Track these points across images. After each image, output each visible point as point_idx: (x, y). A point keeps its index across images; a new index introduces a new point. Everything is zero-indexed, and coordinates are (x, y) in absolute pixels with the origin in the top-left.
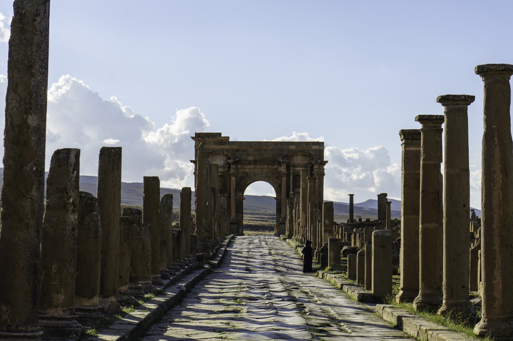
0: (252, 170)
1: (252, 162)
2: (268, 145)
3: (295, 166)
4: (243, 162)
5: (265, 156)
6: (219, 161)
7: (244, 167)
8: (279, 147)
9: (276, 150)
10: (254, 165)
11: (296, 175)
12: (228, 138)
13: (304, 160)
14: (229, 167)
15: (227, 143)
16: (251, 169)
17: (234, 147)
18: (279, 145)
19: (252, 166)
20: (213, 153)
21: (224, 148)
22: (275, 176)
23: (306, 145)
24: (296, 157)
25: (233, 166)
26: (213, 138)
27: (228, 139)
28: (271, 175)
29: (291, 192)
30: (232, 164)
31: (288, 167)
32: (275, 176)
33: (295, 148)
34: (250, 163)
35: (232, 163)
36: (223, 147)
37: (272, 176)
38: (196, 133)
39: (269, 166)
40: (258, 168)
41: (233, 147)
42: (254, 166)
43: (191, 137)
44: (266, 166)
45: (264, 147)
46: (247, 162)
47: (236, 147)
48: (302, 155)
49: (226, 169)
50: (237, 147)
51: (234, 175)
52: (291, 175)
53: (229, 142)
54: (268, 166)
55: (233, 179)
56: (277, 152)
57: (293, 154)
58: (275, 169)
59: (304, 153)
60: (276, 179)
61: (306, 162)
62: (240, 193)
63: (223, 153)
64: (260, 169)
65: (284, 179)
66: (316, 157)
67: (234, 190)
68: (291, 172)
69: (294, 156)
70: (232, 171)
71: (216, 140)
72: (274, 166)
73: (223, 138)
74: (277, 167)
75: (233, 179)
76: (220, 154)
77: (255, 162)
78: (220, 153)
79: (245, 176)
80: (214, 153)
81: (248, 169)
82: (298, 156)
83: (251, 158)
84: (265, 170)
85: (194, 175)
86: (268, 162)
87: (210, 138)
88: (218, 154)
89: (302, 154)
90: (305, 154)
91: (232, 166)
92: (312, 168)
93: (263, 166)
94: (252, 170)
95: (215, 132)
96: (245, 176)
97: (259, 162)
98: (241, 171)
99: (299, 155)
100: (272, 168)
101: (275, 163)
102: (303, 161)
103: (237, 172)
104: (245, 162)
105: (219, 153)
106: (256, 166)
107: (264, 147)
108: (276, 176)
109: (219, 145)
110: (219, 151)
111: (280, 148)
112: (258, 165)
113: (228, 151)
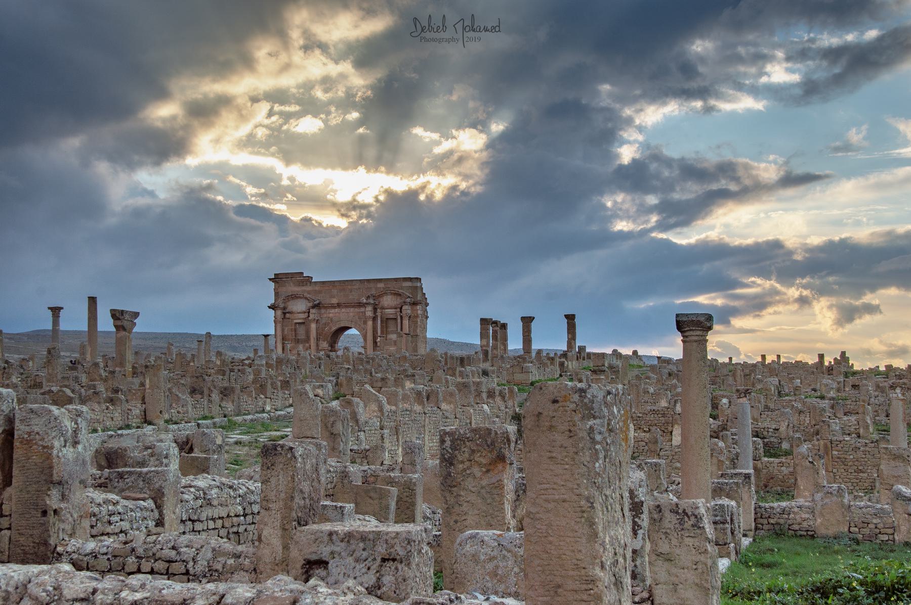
3: (383, 308)
6: (299, 306)
11: (387, 319)
19: (337, 310)
21: (305, 291)
31: (375, 310)
34: (333, 307)
36: (304, 288)
39: (356, 309)
44: (352, 309)
52: (379, 318)
55: (313, 326)
65: (370, 323)
68: (379, 314)
70: (312, 316)
75: (313, 326)
77: (339, 305)
80: (294, 297)
85: (60, 315)
91: (311, 310)
98: (325, 316)
100: (359, 311)
113: (309, 293)
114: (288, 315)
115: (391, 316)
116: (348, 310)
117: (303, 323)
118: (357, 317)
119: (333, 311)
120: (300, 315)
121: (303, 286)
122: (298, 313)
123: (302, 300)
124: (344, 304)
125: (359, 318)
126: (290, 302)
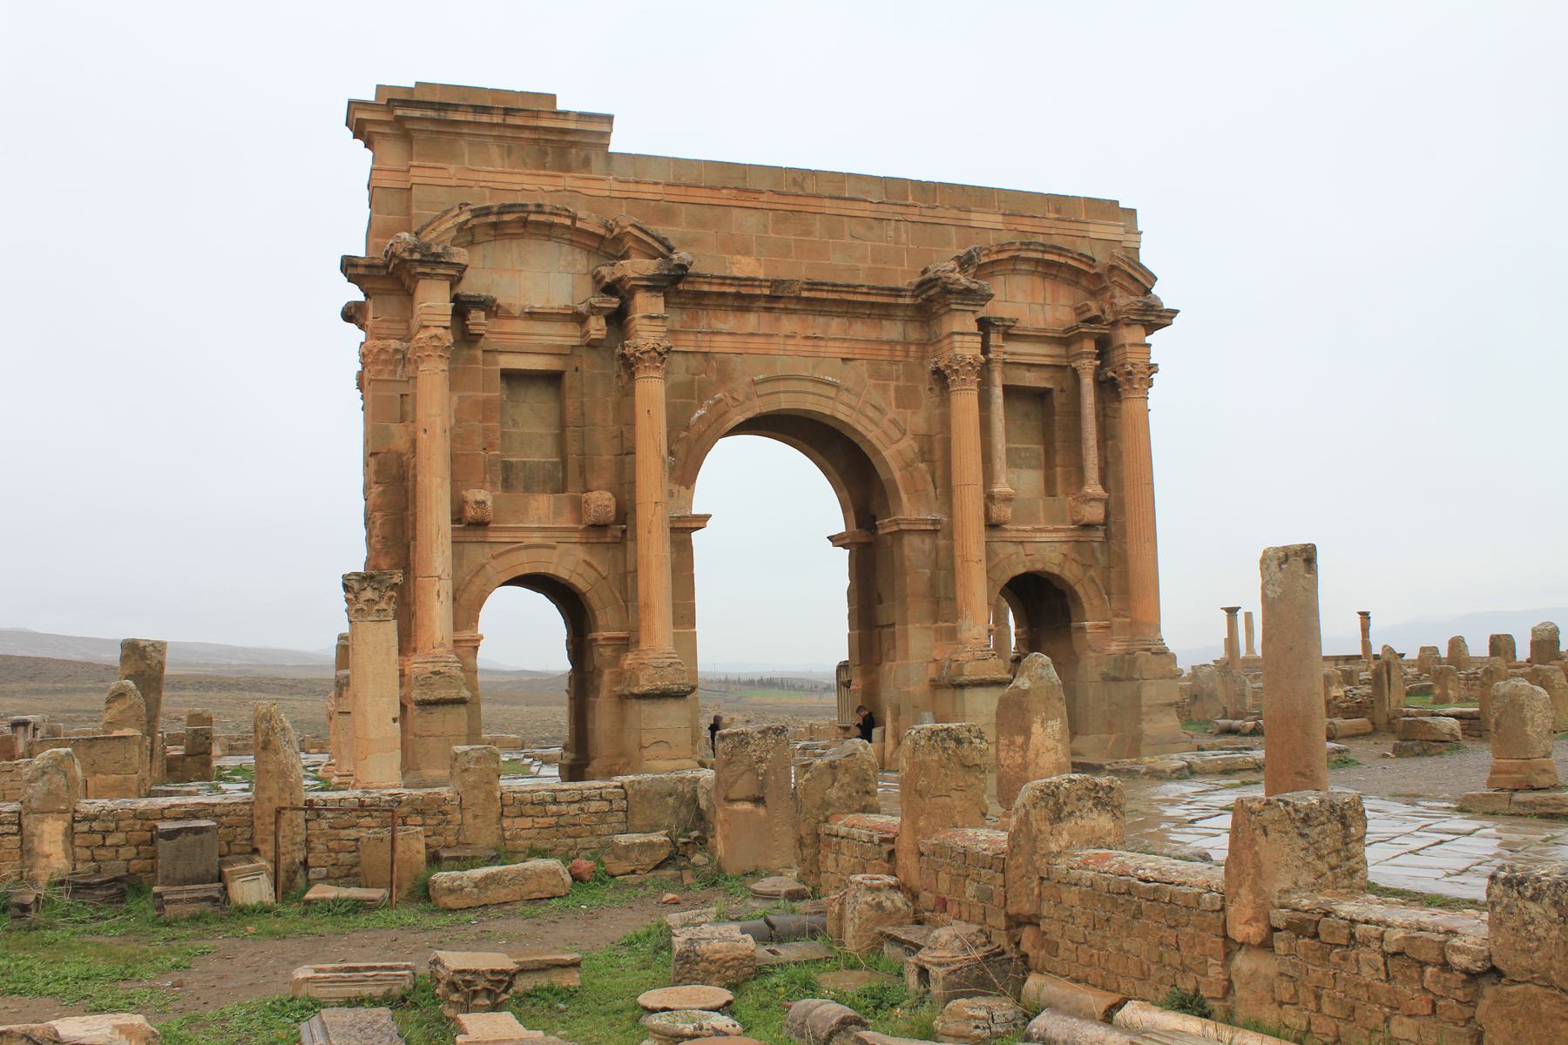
1: (758, 291)
2: (847, 195)
4: (706, 288)
5: (837, 258)
7: (703, 324)
8: (912, 210)
9: (896, 230)
12: (605, 128)
13: (1048, 301)
14: (618, 319)
15: (597, 164)
16: (752, 334)
17: (643, 188)
18: (910, 198)
19: (751, 321)
20: (507, 218)
22: (893, 384)
23: (1058, 211)
24: (1001, 278)
25: (646, 305)
26: (511, 120)
28: (872, 382)
29: (1001, 488)
30: (648, 289)
32: (893, 384)
33: (1000, 226)
34: (741, 298)
35: (648, 279)
36: (569, 181)
37: (876, 385)
38: (379, 87)
39: (860, 329)
41: (632, 187)
42: (765, 316)
44: (835, 326)
45: (827, 202)
46: (732, 290)
47: (652, 188)
48: (1032, 273)
49: (597, 327)
50: (660, 189)
53: (610, 156)
54: (850, 325)
56: (903, 238)
57: (995, 257)
58: (889, 342)
59: (1055, 258)
60: (898, 406)
61: (1058, 314)
63: (574, 218)
64: (807, 338)
65: (965, 401)
66: (1137, 276)
69: (992, 274)
71: (526, 135)
72: (885, 323)
73: (572, 126)
74: (901, 330)
75: (652, 390)
76: (547, 231)
78: (557, 220)
79: (714, 377)
81: (730, 334)
82: (1014, 271)
83: (745, 266)
84: (836, 349)
87: (485, 119)
88: (537, 223)
89: (1037, 261)
90: (1062, 260)
92: (1104, 347)
93: (821, 320)
94: (757, 344)
95: (518, 89)
97: (805, 294)
99: (1024, 267)
100: (873, 335)
101: (901, 301)
102: (1043, 305)
104: (715, 289)
105: (542, 218)
106: (778, 319)
108: (897, 389)
109: (545, 168)
111: (916, 218)
112: (787, 311)
115: (1031, 379)
116: (817, 325)
117: (553, 379)
118: (862, 368)
119: (730, 322)
120: (540, 327)
121: (568, 169)
122: (532, 315)
123: (552, 247)
124: (813, 285)
125: (876, 374)
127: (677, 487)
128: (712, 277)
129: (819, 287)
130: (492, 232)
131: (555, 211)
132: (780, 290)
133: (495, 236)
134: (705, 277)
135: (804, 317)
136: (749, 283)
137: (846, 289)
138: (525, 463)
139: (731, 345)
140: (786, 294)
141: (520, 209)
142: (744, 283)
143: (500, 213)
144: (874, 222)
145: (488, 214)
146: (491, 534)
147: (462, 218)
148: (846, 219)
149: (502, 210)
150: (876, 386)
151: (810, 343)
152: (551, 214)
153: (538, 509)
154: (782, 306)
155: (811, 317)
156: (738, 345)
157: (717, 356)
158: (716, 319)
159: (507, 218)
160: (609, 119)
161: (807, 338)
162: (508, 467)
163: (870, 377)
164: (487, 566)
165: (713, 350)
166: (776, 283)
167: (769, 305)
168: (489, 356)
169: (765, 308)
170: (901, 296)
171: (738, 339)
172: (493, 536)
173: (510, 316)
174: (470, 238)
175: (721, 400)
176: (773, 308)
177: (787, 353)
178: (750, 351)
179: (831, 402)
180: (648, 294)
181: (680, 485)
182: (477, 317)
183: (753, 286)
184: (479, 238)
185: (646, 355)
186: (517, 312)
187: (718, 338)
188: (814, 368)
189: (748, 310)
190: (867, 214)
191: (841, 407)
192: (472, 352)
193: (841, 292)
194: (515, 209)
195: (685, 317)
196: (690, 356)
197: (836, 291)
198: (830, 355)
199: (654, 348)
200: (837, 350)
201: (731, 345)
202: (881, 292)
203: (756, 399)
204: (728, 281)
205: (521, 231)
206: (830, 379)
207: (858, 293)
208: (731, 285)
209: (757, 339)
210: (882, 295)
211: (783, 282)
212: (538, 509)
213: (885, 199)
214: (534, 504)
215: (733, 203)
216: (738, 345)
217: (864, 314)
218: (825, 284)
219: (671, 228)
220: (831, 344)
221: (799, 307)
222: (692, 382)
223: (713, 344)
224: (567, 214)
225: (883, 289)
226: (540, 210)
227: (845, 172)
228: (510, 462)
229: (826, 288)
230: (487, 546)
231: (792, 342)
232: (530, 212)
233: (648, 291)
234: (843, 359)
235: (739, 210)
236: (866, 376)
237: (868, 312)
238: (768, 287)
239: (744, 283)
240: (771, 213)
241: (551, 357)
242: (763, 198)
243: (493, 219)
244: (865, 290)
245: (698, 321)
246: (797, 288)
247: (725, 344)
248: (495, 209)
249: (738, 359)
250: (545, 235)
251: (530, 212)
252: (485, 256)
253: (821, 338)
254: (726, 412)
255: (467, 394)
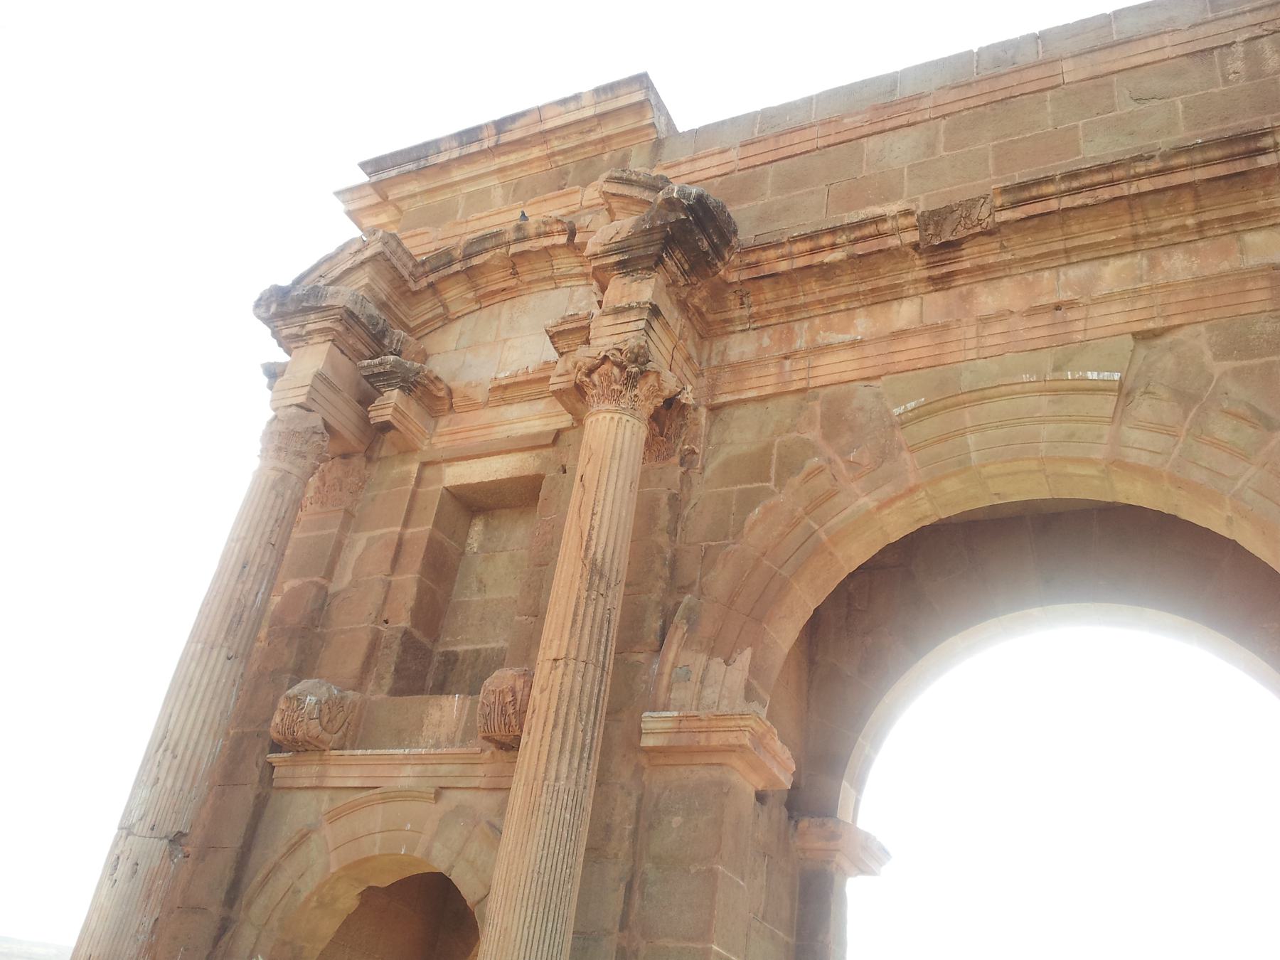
0: (916, 349)
1: (893, 242)
4: (783, 266)
7: (800, 343)
10: (941, 282)
12: (638, 97)
19: (904, 313)
20: (476, 261)
27: (640, 107)
28: (1229, 364)
37: (1237, 374)
39: (1178, 264)
40: (1000, 316)
43: (338, 194)
44: (1111, 274)
46: (838, 255)
50: (732, 155)
51: (632, 381)
54: (1153, 264)
62: (717, 664)
64: (1034, 311)
67: (595, 571)
71: (536, 152)
72: (1254, 239)
78: (546, 242)
79: (813, 435)
81: (853, 344)
84: (1115, 317)
86: (1146, 185)
96: (813, 435)
98: (763, 382)
103: (714, 409)
104: (801, 262)
106: (965, 298)
107: (1067, 66)
110: (531, 228)
112: (985, 272)
114: (390, 403)
119: (863, 324)
126: (457, 327)
127: (702, 658)
128: (794, 240)
129: (1034, 192)
130: (471, 295)
131: (543, 229)
132: (947, 228)
133: (478, 300)
134: (779, 245)
135: (1030, 277)
136: (871, 230)
137: (1103, 177)
138: (478, 652)
139: (854, 365)
140: (964, 233)
141: (494, 242)
142: (858, 234)
143: (467, 256)
144: (1185, 60)
145: (450, 263)
146: (333, 771)
147: (368, 253)
148: (1115, 78)
149: (469, 251)
150: (1237, 374)
151: (1045, 319)
152: (539, 236)
153: (439, 724)
154: (967, 265)
155: (1046, 274)
156: (869, 363)
157: (823, 392)
158: (829, 328)
159: (476, 261)
160: (642, 81)
161: (1034, 311)
162: (451, 660)
163: (1216, 357)
164: (314, 836)
165: (812, 383)
166: (932, 219)
167: (936, 272)
168: (429, 472)
169: (931, 279)
170: (1263, 151)
171: (869, 350)
172: (336, 777)
173: (474, 406)
174: (440, 310)
175: (820, 470)
176: (950, 275)
177: (987, 353)
178: (898, 368)
179: (1106, 430)
180: (627, 280)
181: (712, 653)
182: (390, 403)
183: (880, 235)
184: (454, 308)
185: (595, 377)
186: (481, 396)
187: (828, 359)
188: (1057, 368)
189: (893, 294)
190: (1168, 52)
191: (1134, 436)
192: (405, 468)
193: (1093, 187)
194: (488, 245)
195: (766, 341)
196: (770, 404)
197: (1078, 190)
198: (1100, 333)
199: (606, 357)
200: (1117, 319)
201: (854, 365)
202: (1198, 157)
203: (906, 455)
204: (825, 241)
205: (512, 282)
206: (1092, 375)
207: (1138, 177)
208: (834, 246)
209: (912, 343)
210: (1207, 163)
211: (950, 210)
212: (439, 724)
213: (1210, 16)
214: (434, 715)
215: (865, 131)
216: (869, 363)
217: (1184, 227)
218: (1049, 180)
219: (745, 206)
220: (1096, 311)
221: (1008, 256)
222: (767, 450)
223: (814, 373)
224: (559, 227)
225: (1203, 147)
226: (520, 235)
227: (1108, 11)
228: (455, 654)
229: (1050, 189)
230: (325, 796)
231: (998, 328)
232: (508, 244)
233: (627, 274)
234: (1135, 335)
235: (876, 138)
236: (1208, 356)
237: (1190, 221)
238: (915, 227)
239: (858, 234)
240: (944, 122)
241: (526, 455)
242: (926, 103)
243: (457, 267)
244: (1154, 166)
245: (790, 341)
246: (984, 212)
247: (843, 367)
248: (458, 253)
249: (862, 392)
250: (544, 279)
251: (508, 244)
252: (461, 334)
253: (1071, 304)
254: (832, 494)
255: (378, 532)
